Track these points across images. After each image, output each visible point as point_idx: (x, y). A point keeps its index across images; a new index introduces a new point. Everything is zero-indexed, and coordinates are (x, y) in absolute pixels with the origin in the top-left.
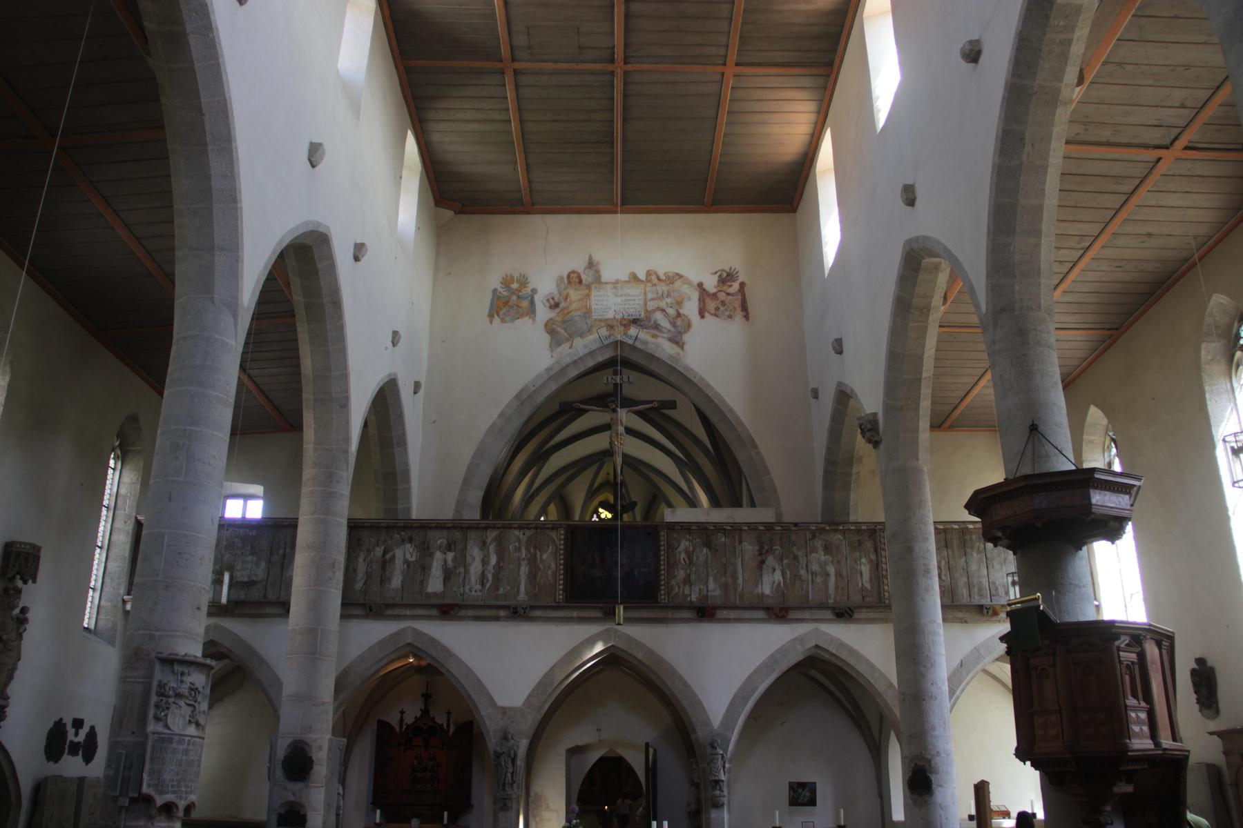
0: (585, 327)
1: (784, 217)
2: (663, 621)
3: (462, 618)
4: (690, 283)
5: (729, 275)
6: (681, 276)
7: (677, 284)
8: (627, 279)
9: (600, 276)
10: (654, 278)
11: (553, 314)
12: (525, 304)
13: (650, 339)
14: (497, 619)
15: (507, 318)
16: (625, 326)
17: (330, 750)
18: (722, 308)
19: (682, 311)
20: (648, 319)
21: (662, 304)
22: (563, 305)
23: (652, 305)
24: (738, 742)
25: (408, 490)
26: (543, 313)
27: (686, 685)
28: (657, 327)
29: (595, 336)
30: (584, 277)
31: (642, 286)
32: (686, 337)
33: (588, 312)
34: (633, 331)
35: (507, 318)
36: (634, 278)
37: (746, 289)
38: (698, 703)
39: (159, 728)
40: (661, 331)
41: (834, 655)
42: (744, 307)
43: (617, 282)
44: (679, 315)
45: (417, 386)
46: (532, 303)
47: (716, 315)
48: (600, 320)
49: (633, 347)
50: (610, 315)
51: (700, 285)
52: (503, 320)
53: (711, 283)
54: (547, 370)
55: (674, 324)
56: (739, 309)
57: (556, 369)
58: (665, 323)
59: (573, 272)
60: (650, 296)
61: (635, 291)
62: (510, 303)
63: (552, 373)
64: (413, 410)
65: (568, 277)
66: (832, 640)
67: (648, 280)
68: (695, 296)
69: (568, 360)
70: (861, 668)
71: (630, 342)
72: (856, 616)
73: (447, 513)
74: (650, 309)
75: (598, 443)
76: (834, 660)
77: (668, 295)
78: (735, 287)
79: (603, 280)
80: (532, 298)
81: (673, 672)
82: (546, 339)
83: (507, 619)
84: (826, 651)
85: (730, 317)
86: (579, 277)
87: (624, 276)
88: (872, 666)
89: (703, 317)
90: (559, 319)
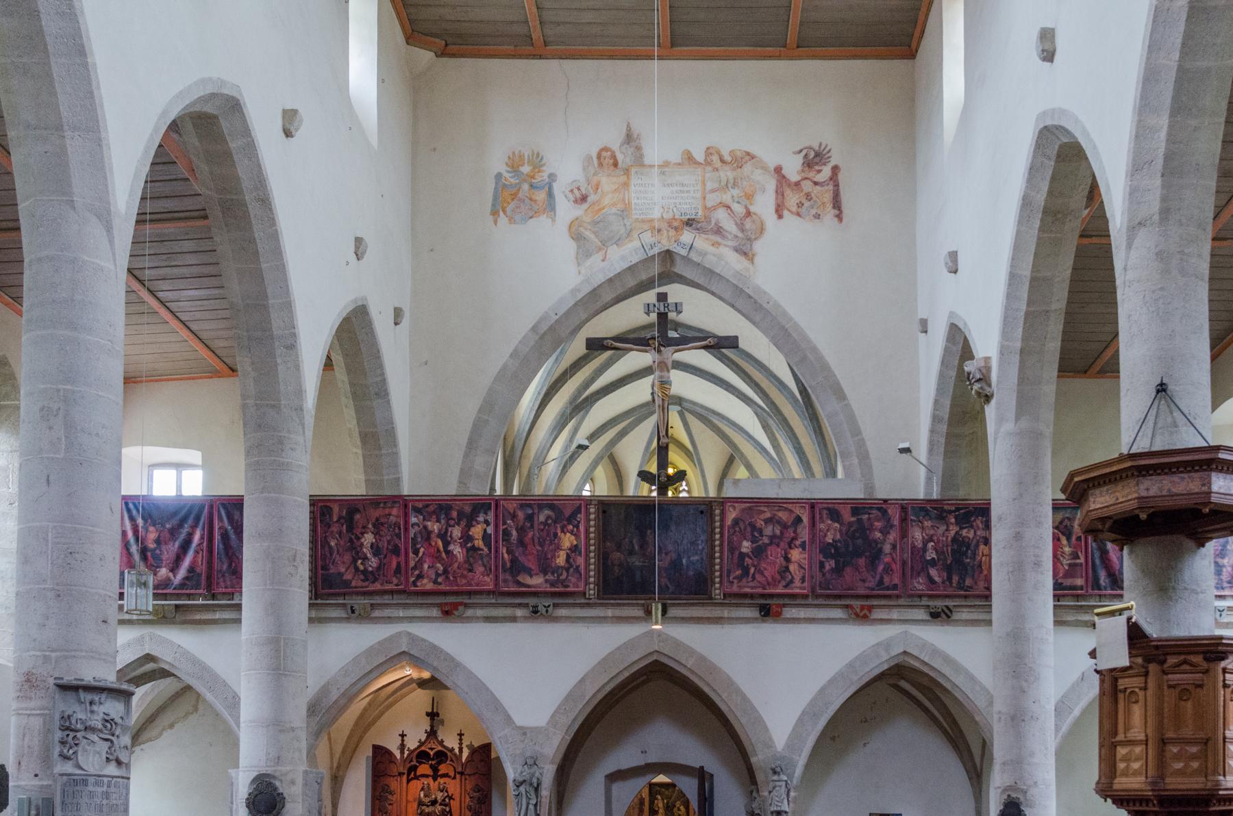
0: (623, 231)
1: (897, 66)
2: (718, 620)
3: (469, 619)
4: (764, 168)
5: (817, 154)
6: (753, 157)
7: (748, 168)
8: (679, 161)
9: (642, 156)
10: (715, 158)
11: (579, 211)
12: (541, 196)
13: (711, 249)
14: (514, 619)
15: (517, 217)
16: (676, 229)
17: (305, 785)
18: (807, 204)
19: (752, 209)
20: (708, 219)
21: (726, 198)
22: (589, 199)
23: (712, 199)
24: (807, 766)
25: (395, 455)
26: (566, 210)
27: (745, 698)
28: (719, 231)
29: (637, 244)
30: (620, 157)
31: (699, 171)
32: (758, 246)
33: (625, 211)
34: (687, 236)
35: (517, 217)
36: (689, 158)
37: (841, 177)
38: (759, 721)
39: (68, 768)
40: (724, 237)
41: (926, 664)
42: (837, 204)
43: (666, 164)
44: (749, 214)
45: (398, 314)
46: (550, 194)
47: (798, 214)
48: (643, 221)
49: (686, 259)
50: (656, 214)
51: (778, 170)
52: (511, 220)
53: (793, 168)
54: (574, 291)
55: (742, 228)
56: (829, 206)
57: (587, 289)
58: (730, 226)
59: (605, 149)
60: (709, 186)
61: (690, 178)
62: (521, 193)
63: (580, 296)
64: (394, 349)
65: (599, 157)
66: (924, 645)
67: (708, 163)
68: (771, 185)
69: (600, 278)
70: (959, 680)
71: (684, 252)
72: (956, 616)
73: (448, 487)
74: (709, 204)
75: (640, 392)
76: (926, 670)
77: (735, 185)
78: (826, 172)
79: (647, 161)
80: (550, 188)
81: (730, 683)
82: (571, 246)
83: (526, 619)
84: (917, 658)
85: (817, 216)
86: (614, 157)
87: (675, 157)
88: (972, 678)
89: (780, 217)
90: (589, 220)
